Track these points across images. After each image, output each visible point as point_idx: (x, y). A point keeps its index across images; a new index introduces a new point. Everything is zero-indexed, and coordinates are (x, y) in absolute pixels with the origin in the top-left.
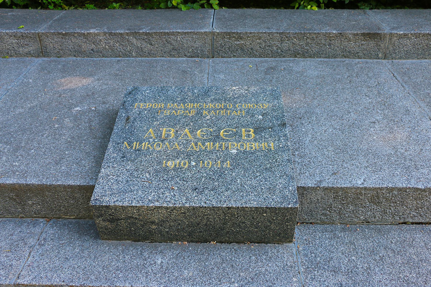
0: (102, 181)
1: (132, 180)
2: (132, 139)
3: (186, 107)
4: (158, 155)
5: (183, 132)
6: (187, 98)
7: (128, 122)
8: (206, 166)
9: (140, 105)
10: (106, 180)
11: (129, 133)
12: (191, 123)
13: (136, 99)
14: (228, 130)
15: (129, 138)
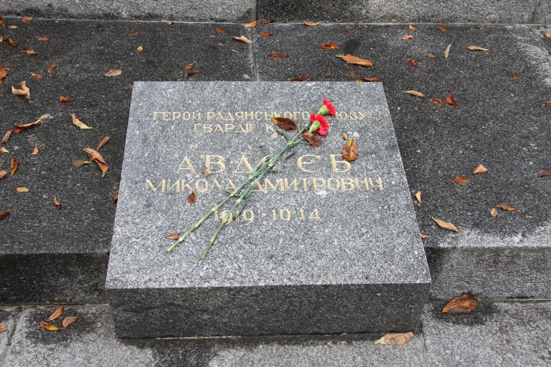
0: (119, 248)
1: (168, 244)
2: (158, 174)
3: (237, 118)
5: (237, 162)
6: (237, 103)
7: (146, 144)
8: (282, 218)
9: (162, 115)
10: (126, 245)
11: (151, 164)
12: (248, 145)
13: (152, 103)
14: (309, 157)
15: (153, 173)
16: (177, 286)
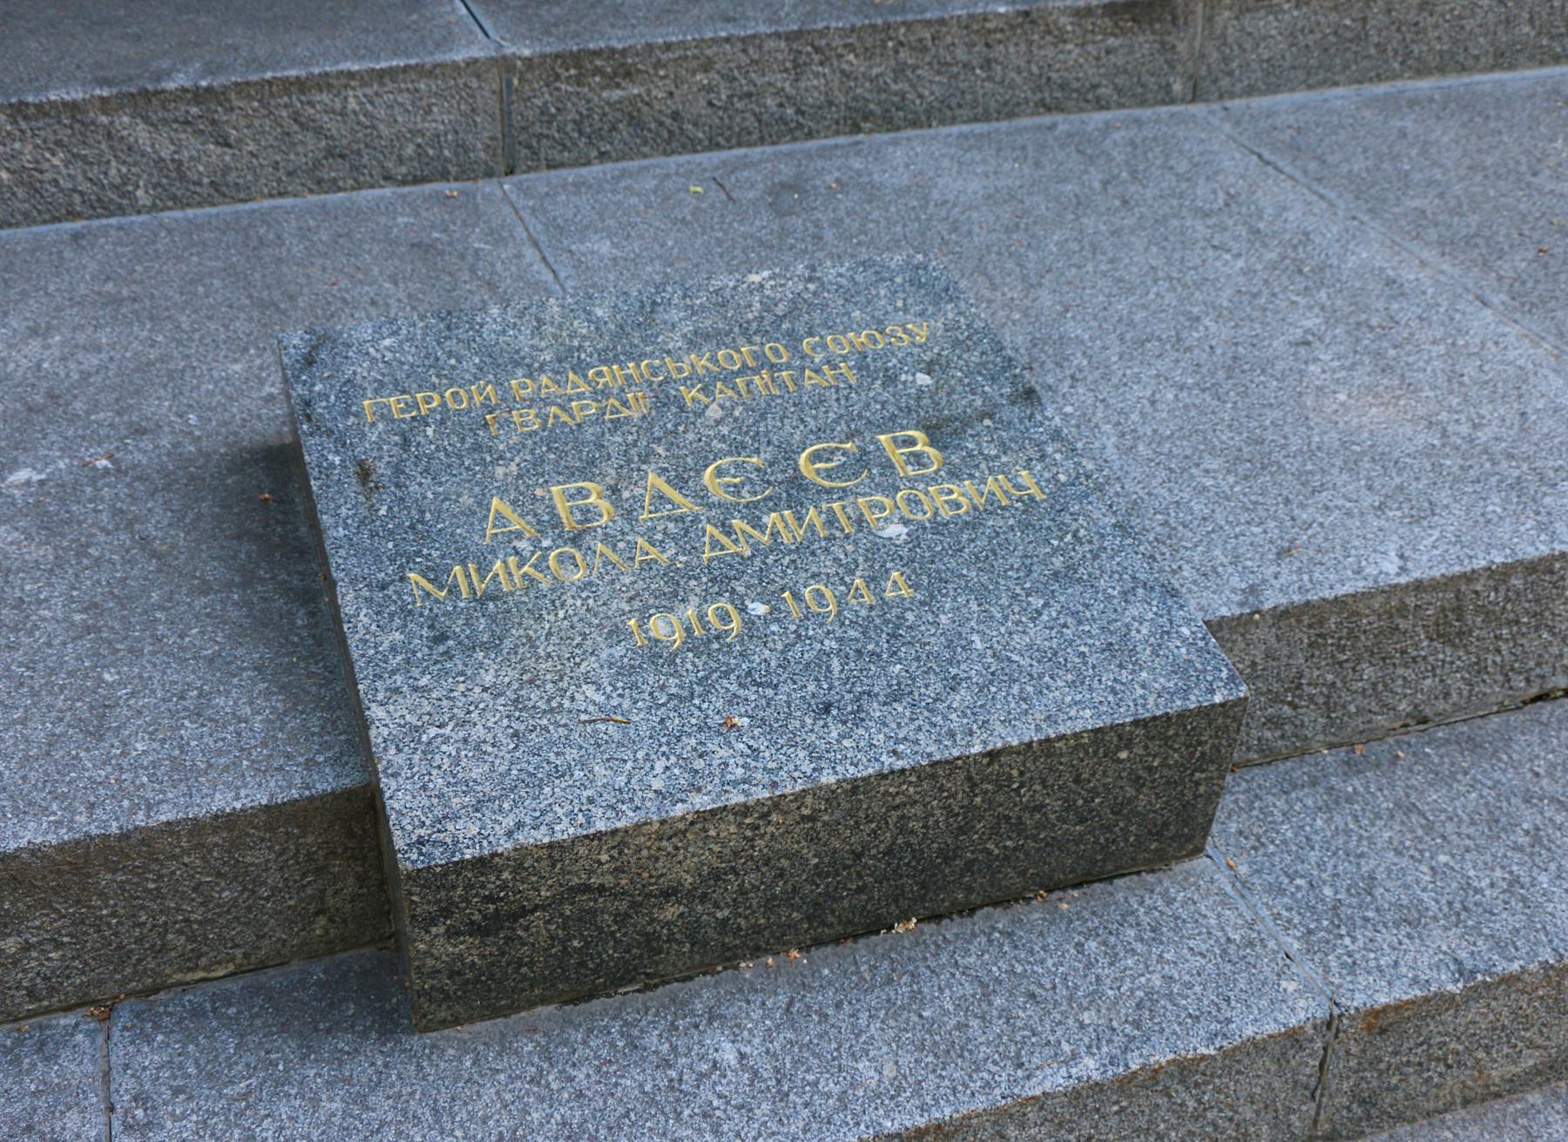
4: (591, 602)
16: (601, 826)
